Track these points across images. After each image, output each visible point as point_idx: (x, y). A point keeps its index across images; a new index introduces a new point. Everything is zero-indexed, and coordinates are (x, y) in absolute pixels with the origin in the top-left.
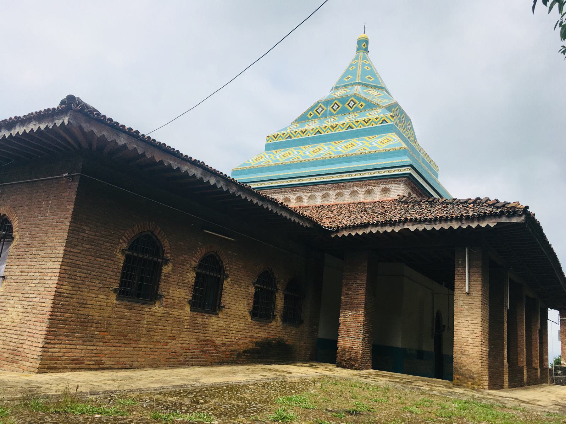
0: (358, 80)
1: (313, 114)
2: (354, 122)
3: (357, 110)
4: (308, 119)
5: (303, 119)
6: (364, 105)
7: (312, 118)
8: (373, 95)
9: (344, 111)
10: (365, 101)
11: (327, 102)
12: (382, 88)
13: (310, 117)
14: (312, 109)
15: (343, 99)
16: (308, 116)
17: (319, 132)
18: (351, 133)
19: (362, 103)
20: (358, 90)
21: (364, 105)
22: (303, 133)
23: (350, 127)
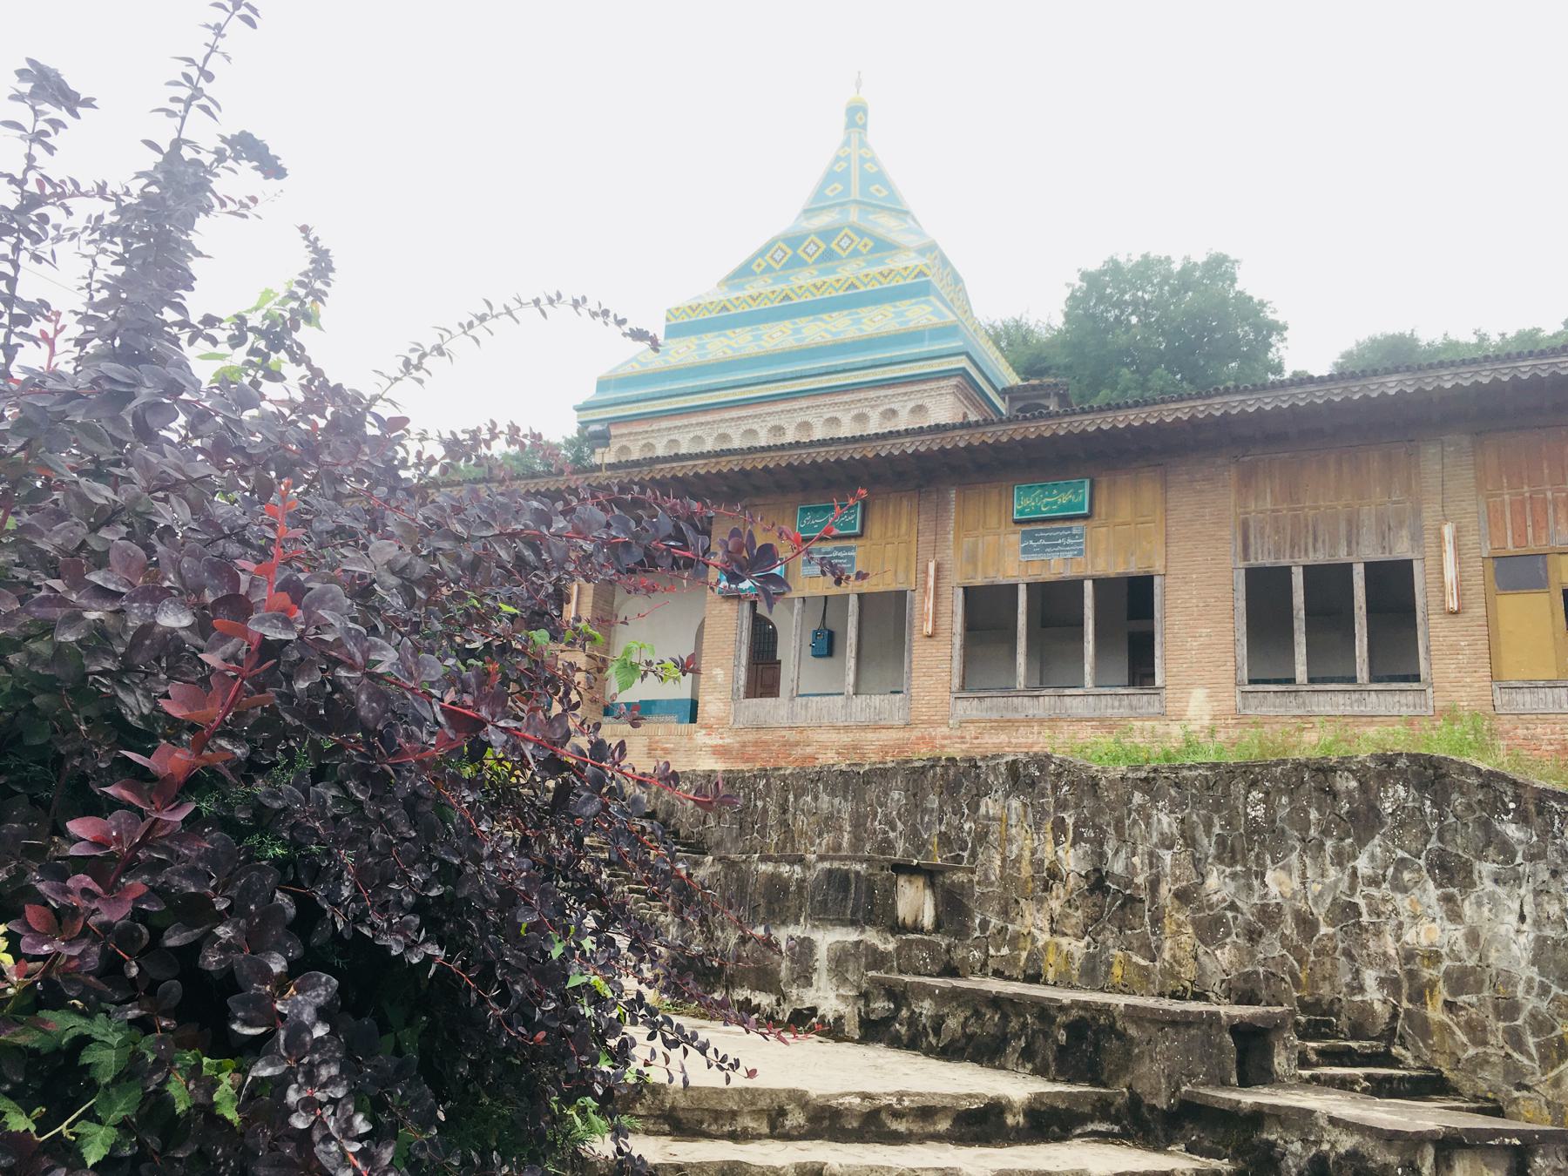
0: (855, 194)
1: (764, 265)
2: (861, 275)
3: (856, 254)
4: (753, 273)
5: (744, 272)
6: (871, 244)
7: (763, 272)
8: (886, 225)
9: (829, 255)
10: (872, 237)
11: (794, 240)
12: (907, 213)
13: (758, 271)
14: (761, 253)
15: (827, 234)
16: (754, 267)
17: (787, 297)
18: (853, 300)
19: (866, 240)
20: (854, 216)
21: (871, 244)
22: (754, 300)
23: (853, 286)
